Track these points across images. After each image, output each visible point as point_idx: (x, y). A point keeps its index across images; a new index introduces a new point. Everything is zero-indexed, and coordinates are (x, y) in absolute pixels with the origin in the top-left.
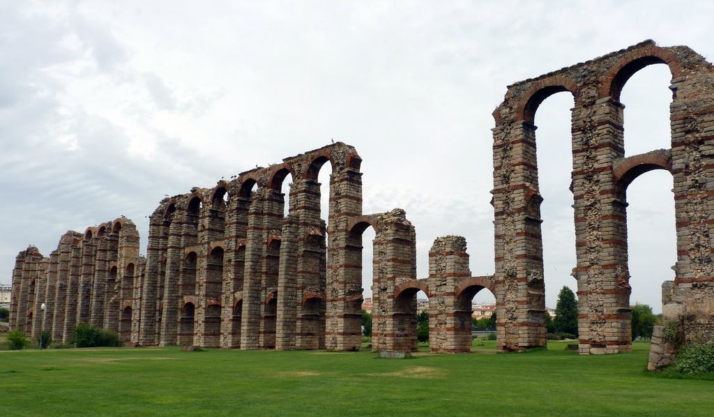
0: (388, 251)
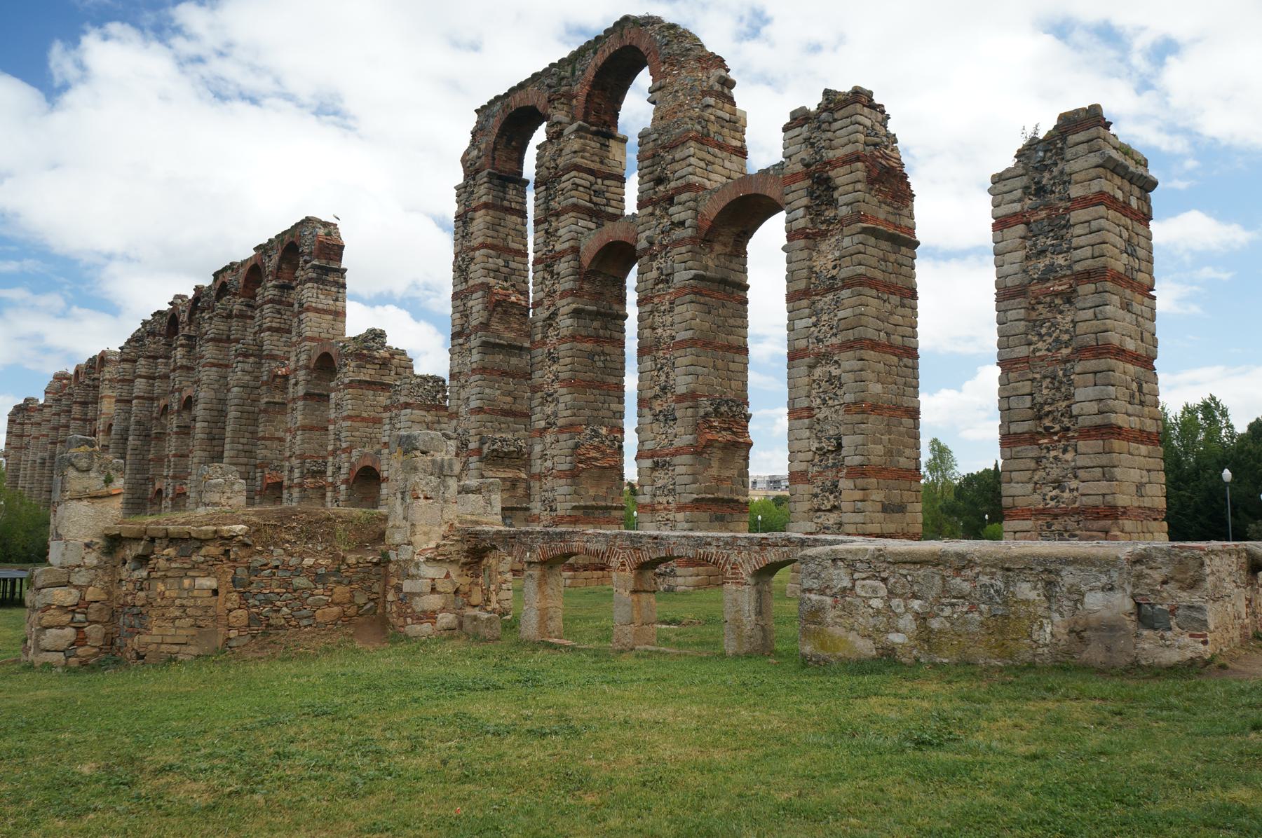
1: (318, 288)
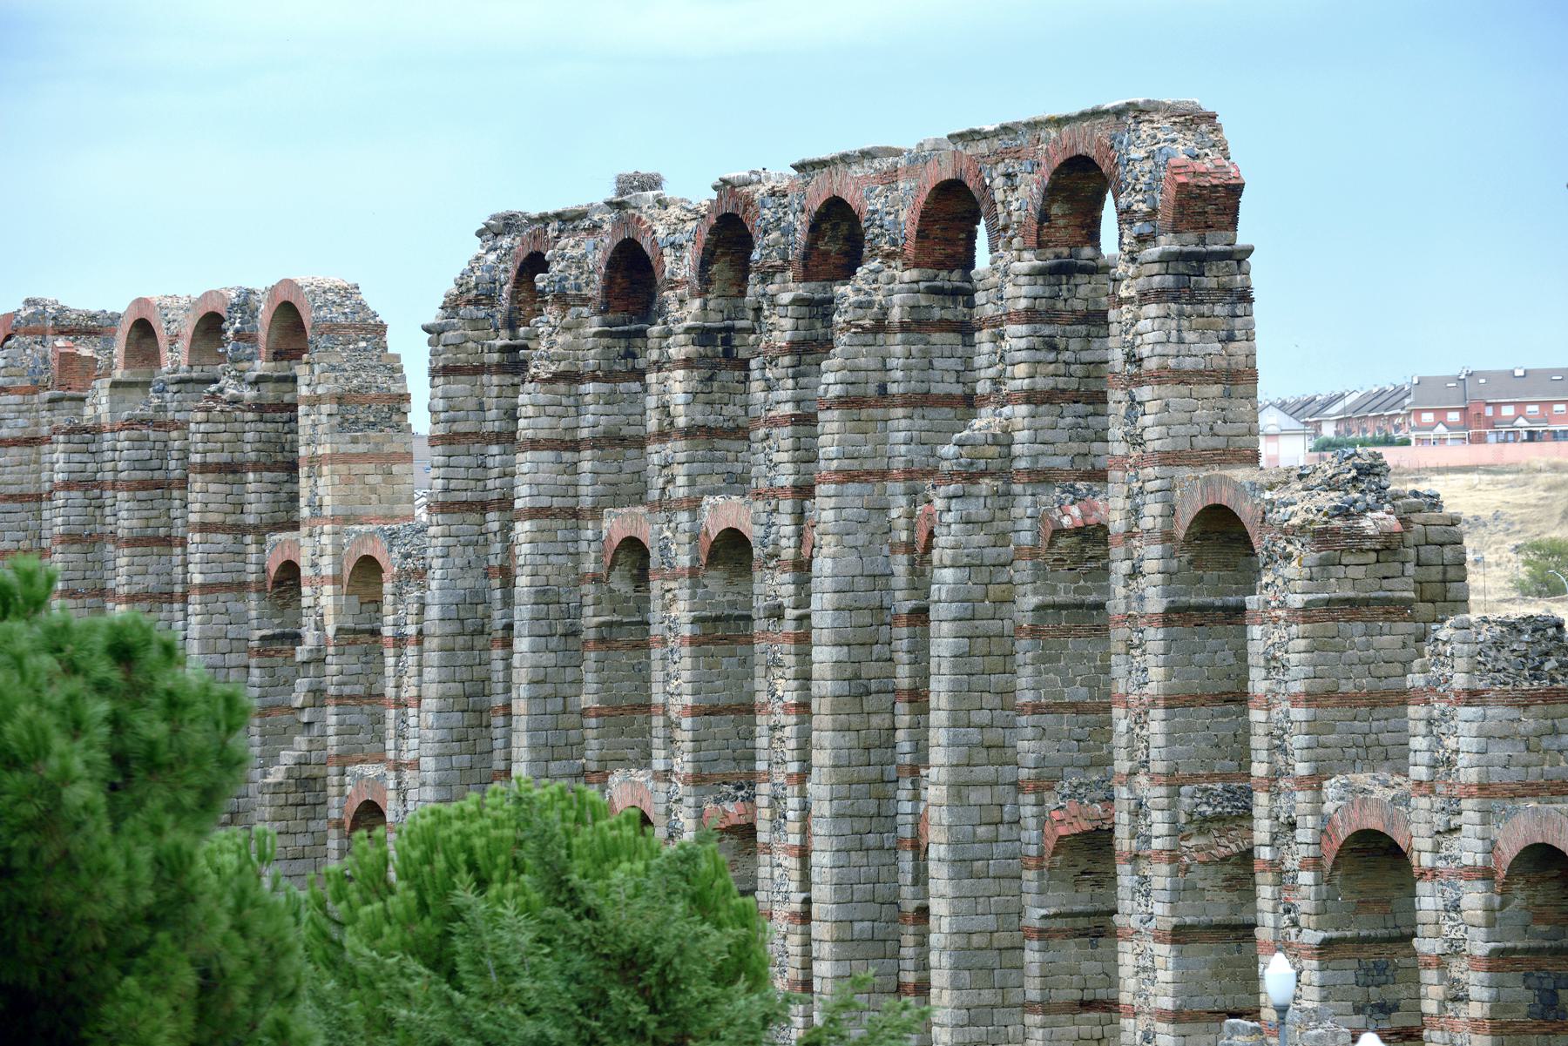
0: (1294, 658)
1: (1180, 314)
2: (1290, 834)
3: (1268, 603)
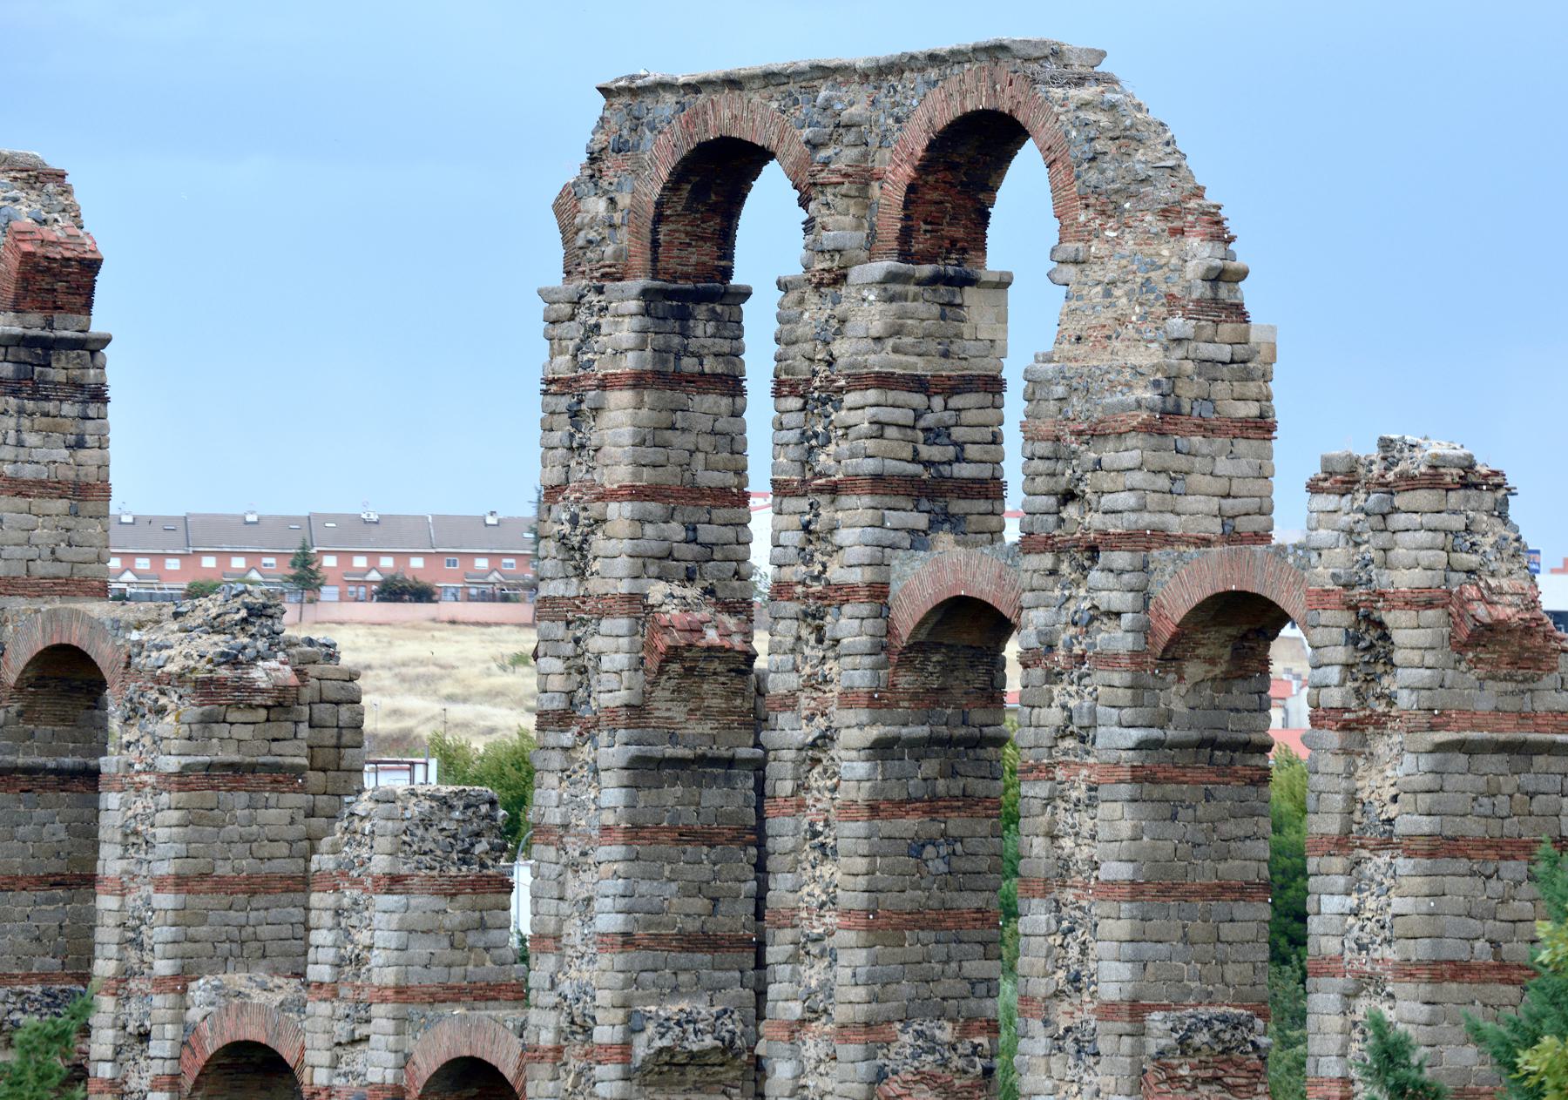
0: (162, 833)
1: (21, 411)
2: (138, 1047)
3: (131, 765)
